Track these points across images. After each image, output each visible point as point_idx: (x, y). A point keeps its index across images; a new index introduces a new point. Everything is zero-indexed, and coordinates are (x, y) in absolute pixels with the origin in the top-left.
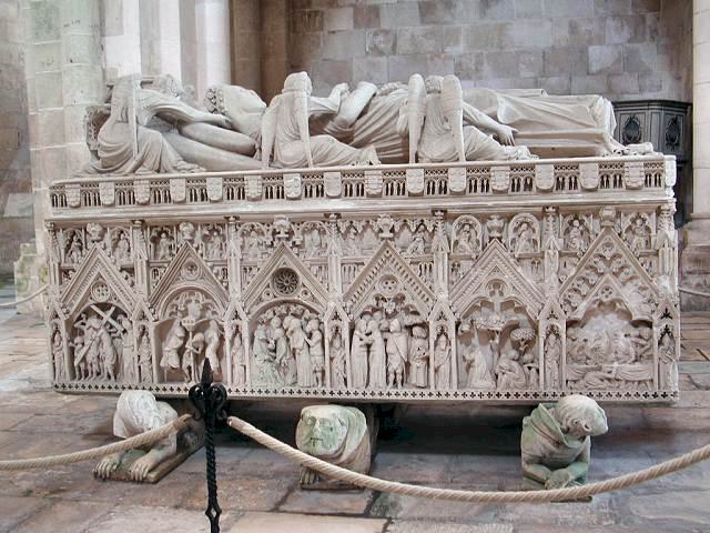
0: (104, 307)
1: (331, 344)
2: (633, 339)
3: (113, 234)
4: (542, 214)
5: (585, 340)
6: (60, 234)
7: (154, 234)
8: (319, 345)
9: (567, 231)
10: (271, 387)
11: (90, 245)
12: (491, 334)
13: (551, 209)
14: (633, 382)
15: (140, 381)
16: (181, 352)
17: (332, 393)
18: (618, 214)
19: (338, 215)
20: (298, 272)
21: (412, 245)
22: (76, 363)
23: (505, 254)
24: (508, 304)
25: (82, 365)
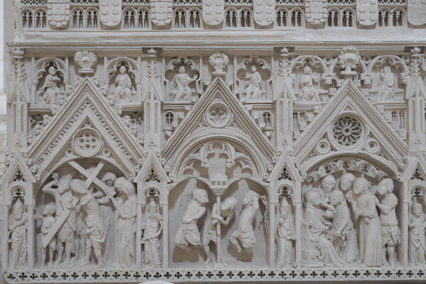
1: (412, 210)
3: (111, 66)
7: (171, 67)
10: (329, 269)
20: (366, 119)
22: (45, 241)
25: (53, 245)
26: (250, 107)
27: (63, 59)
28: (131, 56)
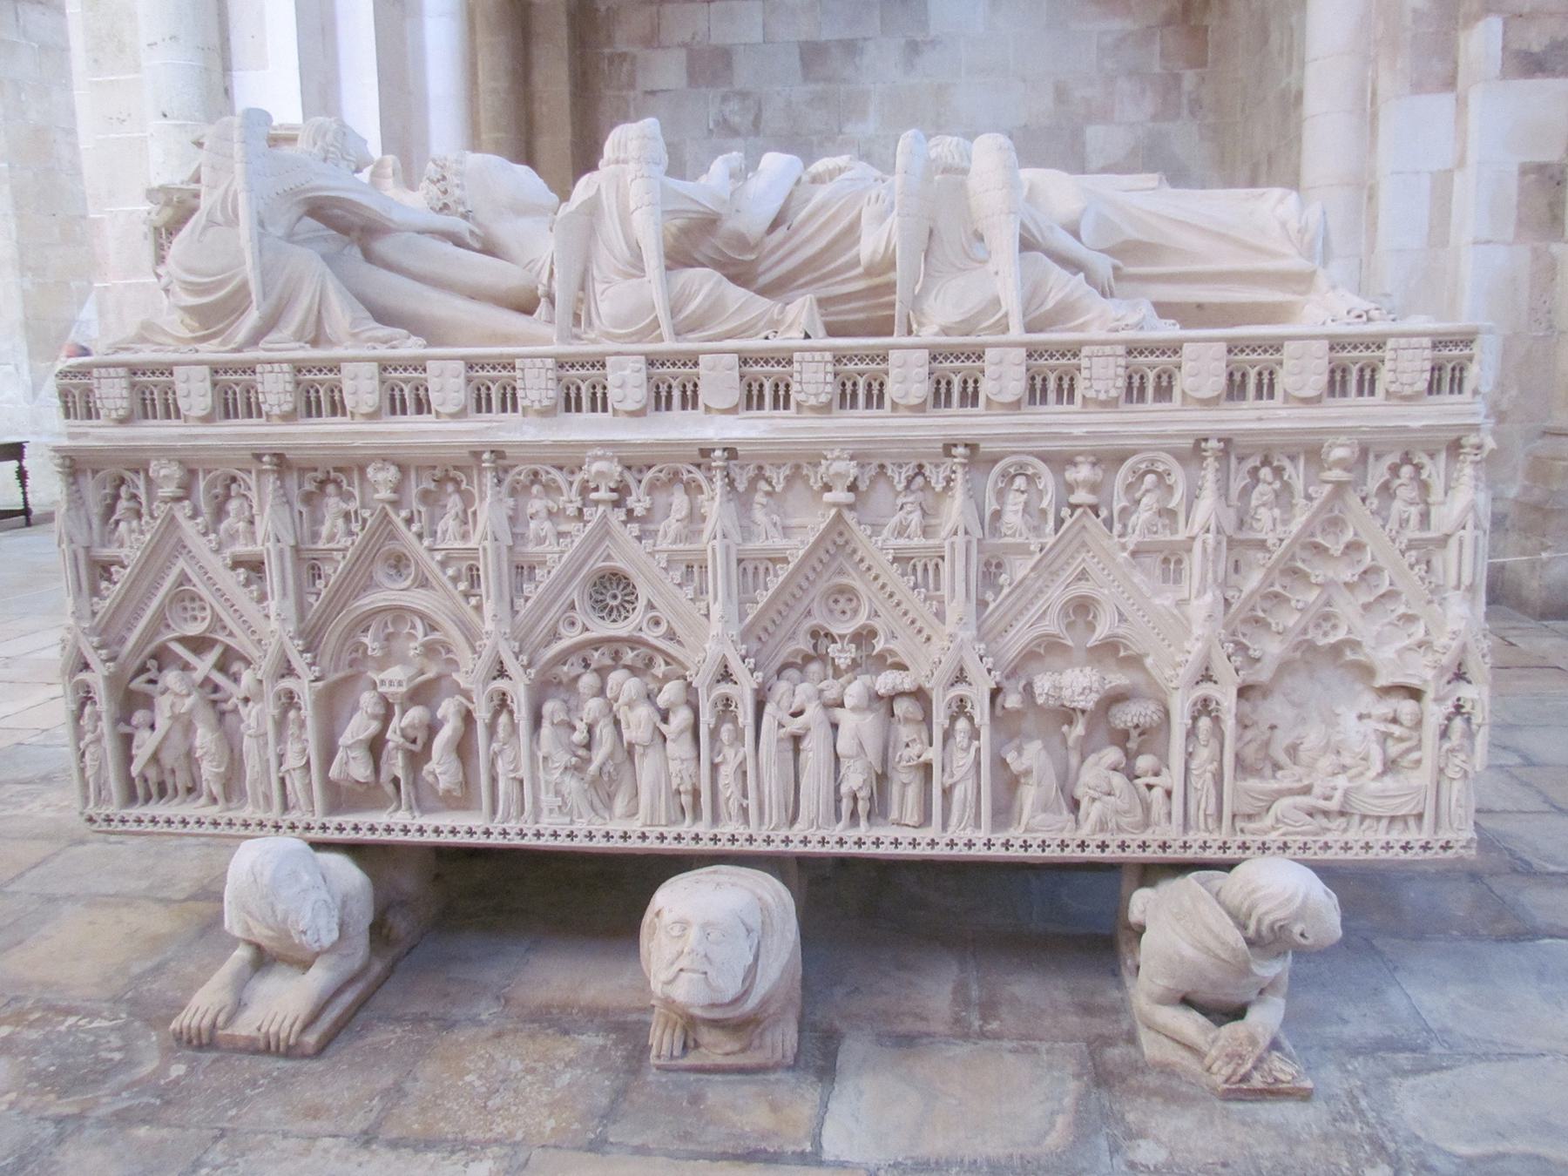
0: (199, 645)
1: (714, 733)
2: (1382, 727)
3: (211, 485)
4: (1194, 453)
5: (1273, 727)
6: (88, 484)
7: (310, 486)
8: (688, 736)
9: (1246, 492)
10: (581, 827)
11: (160, 510)
12: (1067, 715)
13: (1213, 444)
14: (1379, 818)
15: (286, 807)
16: (376, 747)
17: (715, 839)
18: (1364, 452)
19: (731, 452)
21: (894, 521)
22: (135, 770)
23: (1105, 543)
24: (1110, 649)
25: (152, 774)
26: (439, 556)
27: (137, 472)
28: (240, 466)
